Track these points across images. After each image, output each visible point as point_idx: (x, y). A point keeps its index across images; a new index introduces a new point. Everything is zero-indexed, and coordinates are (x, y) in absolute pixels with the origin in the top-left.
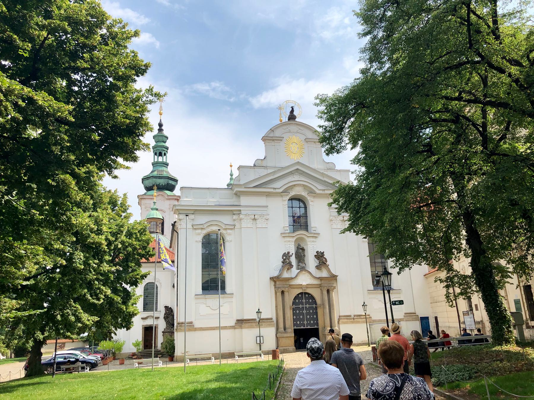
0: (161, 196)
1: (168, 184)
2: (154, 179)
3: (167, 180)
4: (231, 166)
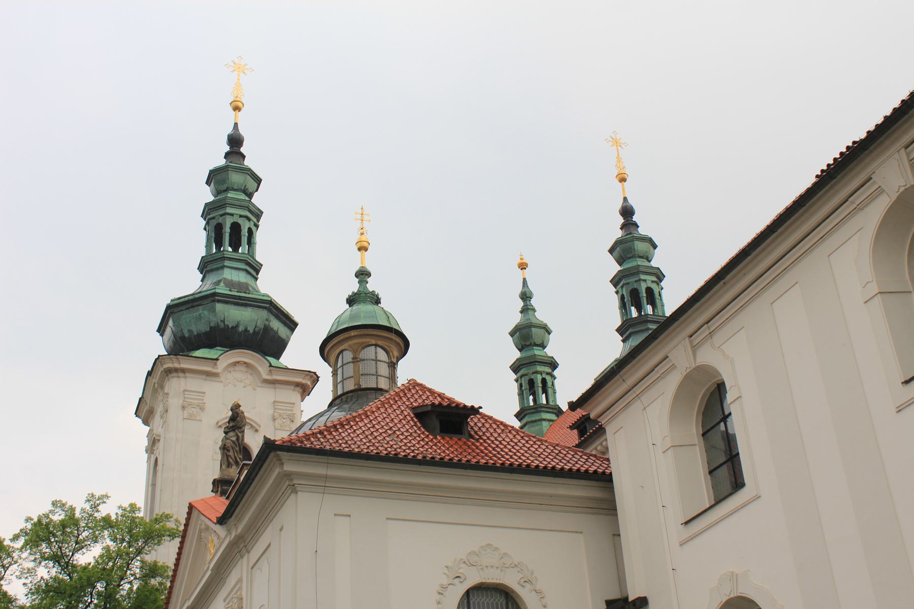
0: (243, 368)
1: (267, 329)
2: (219, 307)
3: (264, 314)
4: (523, 266)
